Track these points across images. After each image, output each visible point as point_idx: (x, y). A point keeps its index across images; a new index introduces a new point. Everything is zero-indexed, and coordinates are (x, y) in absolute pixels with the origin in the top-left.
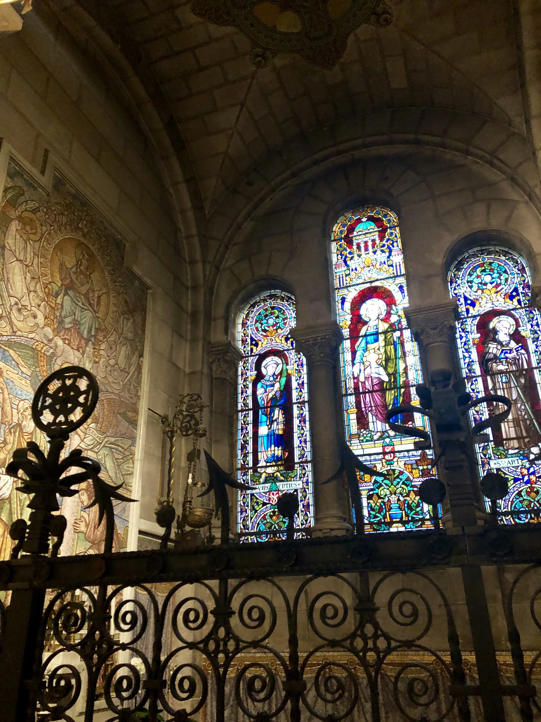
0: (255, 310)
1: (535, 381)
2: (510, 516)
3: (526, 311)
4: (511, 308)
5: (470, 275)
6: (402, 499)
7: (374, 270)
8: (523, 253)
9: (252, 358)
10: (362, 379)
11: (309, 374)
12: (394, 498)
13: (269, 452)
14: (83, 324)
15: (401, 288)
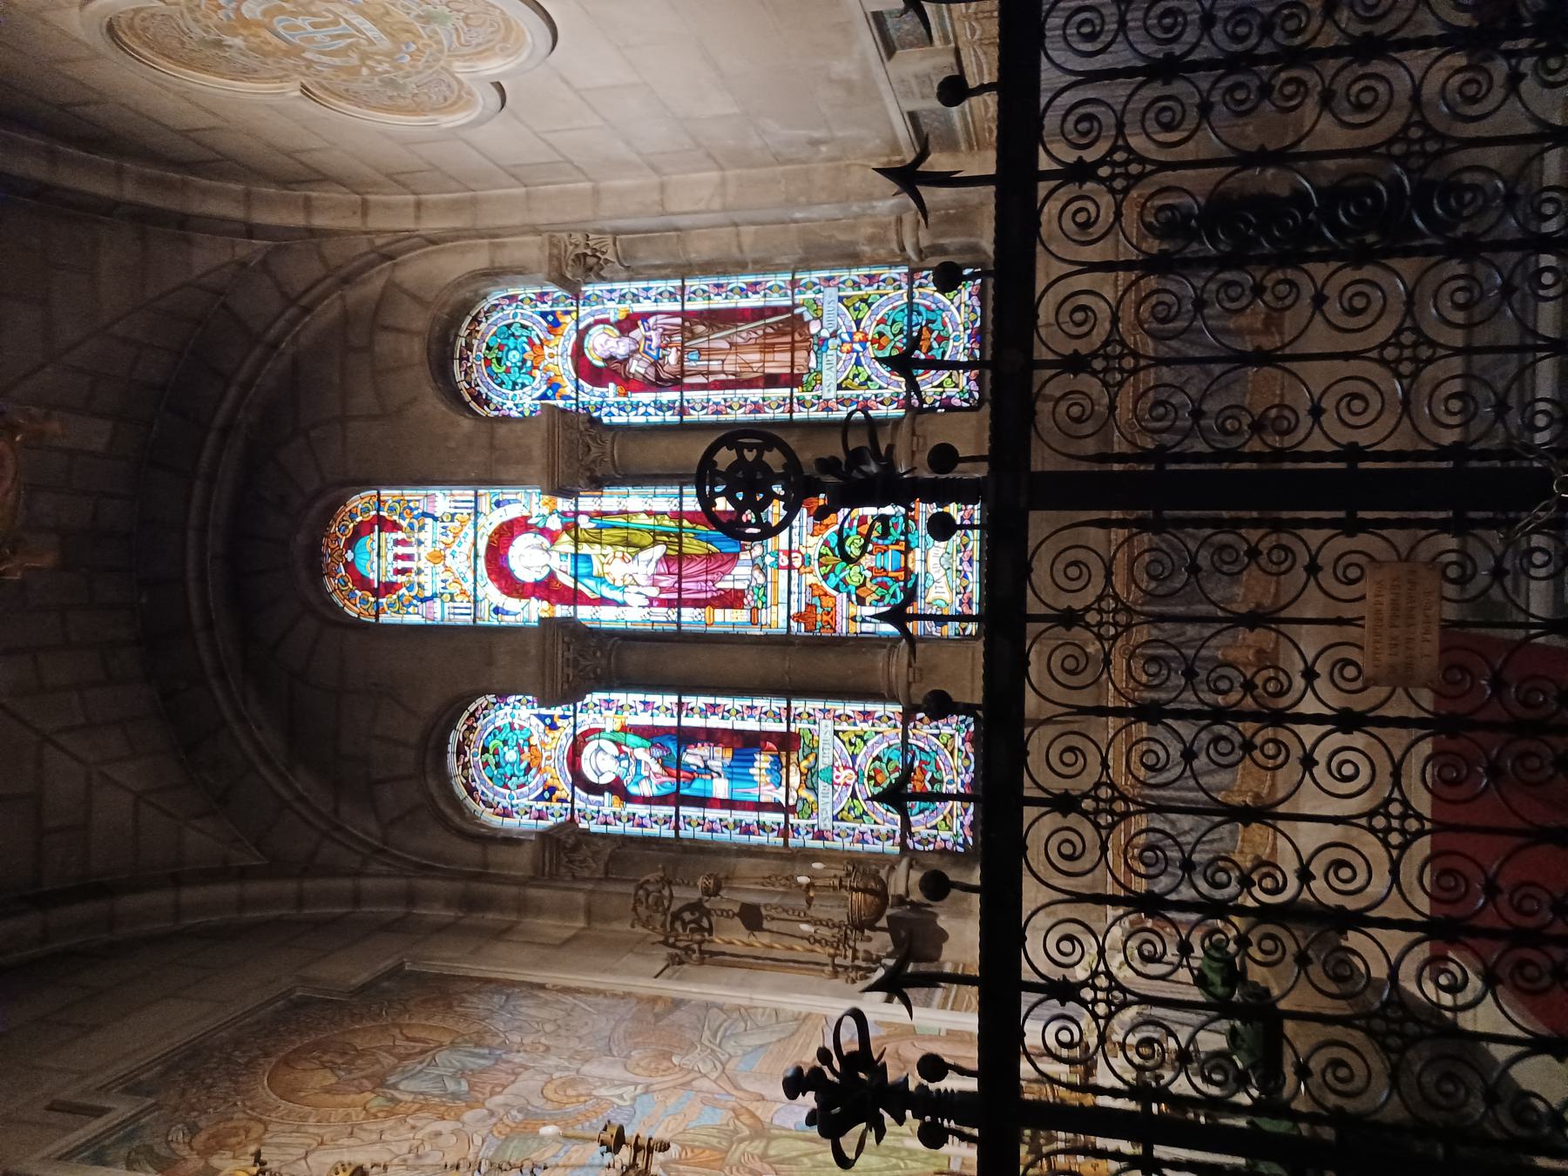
0: (481, 788)
8: (482, 292)
9: (576, 801)
10: (654, 592)
13: (763, 779)
15: (498, 504)
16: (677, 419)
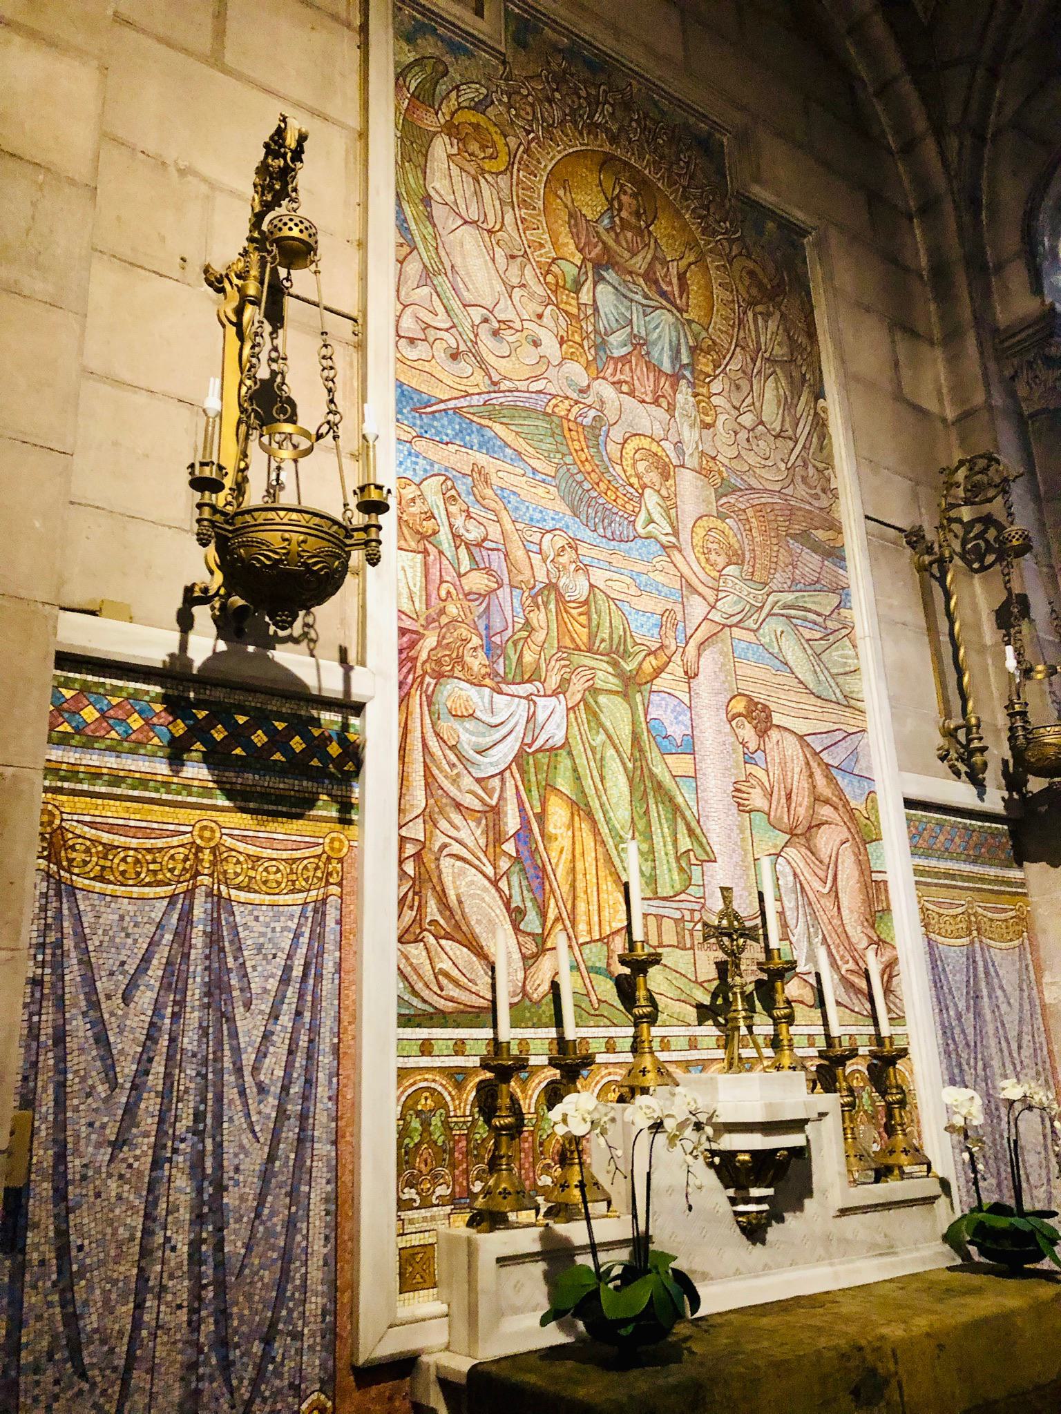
14: (655, 343)
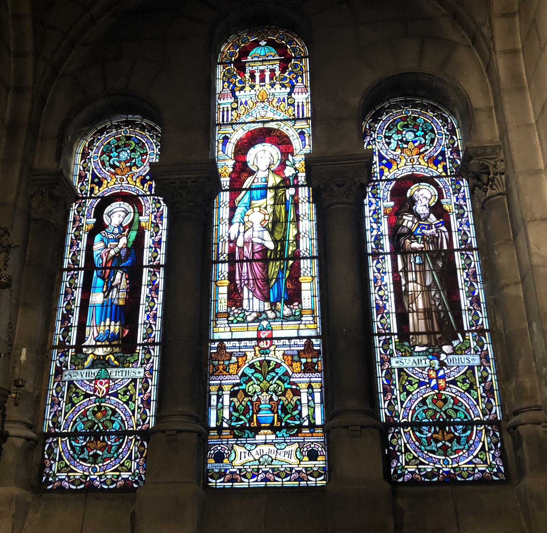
1: (455, 265)
2: (409, 428)
3: (452, 180)
4: (434, 175)
5: (389, 129)
6: (275, 398)
7: (270, 107)
10: (240, 243)
11: (169, 229)
12: (265, 397)
13: (102, 328)
15: (302, 134)
16: (370, 251)
